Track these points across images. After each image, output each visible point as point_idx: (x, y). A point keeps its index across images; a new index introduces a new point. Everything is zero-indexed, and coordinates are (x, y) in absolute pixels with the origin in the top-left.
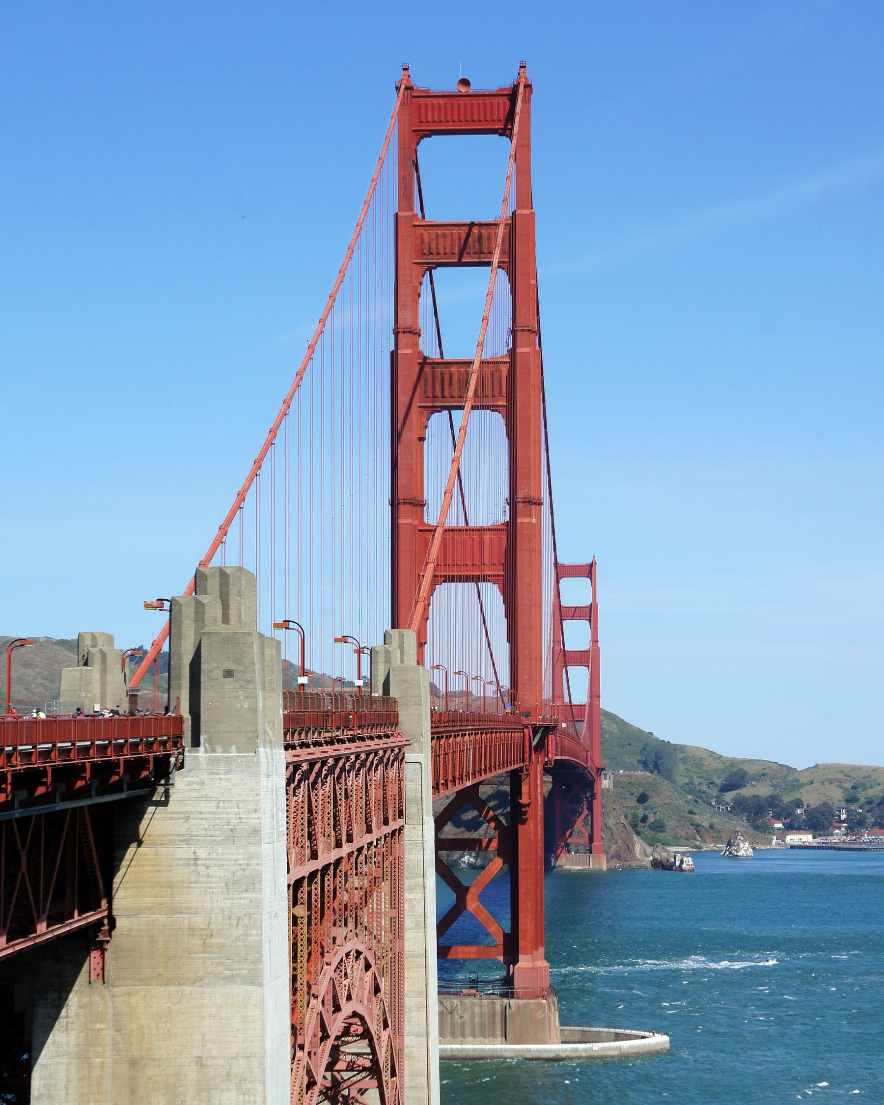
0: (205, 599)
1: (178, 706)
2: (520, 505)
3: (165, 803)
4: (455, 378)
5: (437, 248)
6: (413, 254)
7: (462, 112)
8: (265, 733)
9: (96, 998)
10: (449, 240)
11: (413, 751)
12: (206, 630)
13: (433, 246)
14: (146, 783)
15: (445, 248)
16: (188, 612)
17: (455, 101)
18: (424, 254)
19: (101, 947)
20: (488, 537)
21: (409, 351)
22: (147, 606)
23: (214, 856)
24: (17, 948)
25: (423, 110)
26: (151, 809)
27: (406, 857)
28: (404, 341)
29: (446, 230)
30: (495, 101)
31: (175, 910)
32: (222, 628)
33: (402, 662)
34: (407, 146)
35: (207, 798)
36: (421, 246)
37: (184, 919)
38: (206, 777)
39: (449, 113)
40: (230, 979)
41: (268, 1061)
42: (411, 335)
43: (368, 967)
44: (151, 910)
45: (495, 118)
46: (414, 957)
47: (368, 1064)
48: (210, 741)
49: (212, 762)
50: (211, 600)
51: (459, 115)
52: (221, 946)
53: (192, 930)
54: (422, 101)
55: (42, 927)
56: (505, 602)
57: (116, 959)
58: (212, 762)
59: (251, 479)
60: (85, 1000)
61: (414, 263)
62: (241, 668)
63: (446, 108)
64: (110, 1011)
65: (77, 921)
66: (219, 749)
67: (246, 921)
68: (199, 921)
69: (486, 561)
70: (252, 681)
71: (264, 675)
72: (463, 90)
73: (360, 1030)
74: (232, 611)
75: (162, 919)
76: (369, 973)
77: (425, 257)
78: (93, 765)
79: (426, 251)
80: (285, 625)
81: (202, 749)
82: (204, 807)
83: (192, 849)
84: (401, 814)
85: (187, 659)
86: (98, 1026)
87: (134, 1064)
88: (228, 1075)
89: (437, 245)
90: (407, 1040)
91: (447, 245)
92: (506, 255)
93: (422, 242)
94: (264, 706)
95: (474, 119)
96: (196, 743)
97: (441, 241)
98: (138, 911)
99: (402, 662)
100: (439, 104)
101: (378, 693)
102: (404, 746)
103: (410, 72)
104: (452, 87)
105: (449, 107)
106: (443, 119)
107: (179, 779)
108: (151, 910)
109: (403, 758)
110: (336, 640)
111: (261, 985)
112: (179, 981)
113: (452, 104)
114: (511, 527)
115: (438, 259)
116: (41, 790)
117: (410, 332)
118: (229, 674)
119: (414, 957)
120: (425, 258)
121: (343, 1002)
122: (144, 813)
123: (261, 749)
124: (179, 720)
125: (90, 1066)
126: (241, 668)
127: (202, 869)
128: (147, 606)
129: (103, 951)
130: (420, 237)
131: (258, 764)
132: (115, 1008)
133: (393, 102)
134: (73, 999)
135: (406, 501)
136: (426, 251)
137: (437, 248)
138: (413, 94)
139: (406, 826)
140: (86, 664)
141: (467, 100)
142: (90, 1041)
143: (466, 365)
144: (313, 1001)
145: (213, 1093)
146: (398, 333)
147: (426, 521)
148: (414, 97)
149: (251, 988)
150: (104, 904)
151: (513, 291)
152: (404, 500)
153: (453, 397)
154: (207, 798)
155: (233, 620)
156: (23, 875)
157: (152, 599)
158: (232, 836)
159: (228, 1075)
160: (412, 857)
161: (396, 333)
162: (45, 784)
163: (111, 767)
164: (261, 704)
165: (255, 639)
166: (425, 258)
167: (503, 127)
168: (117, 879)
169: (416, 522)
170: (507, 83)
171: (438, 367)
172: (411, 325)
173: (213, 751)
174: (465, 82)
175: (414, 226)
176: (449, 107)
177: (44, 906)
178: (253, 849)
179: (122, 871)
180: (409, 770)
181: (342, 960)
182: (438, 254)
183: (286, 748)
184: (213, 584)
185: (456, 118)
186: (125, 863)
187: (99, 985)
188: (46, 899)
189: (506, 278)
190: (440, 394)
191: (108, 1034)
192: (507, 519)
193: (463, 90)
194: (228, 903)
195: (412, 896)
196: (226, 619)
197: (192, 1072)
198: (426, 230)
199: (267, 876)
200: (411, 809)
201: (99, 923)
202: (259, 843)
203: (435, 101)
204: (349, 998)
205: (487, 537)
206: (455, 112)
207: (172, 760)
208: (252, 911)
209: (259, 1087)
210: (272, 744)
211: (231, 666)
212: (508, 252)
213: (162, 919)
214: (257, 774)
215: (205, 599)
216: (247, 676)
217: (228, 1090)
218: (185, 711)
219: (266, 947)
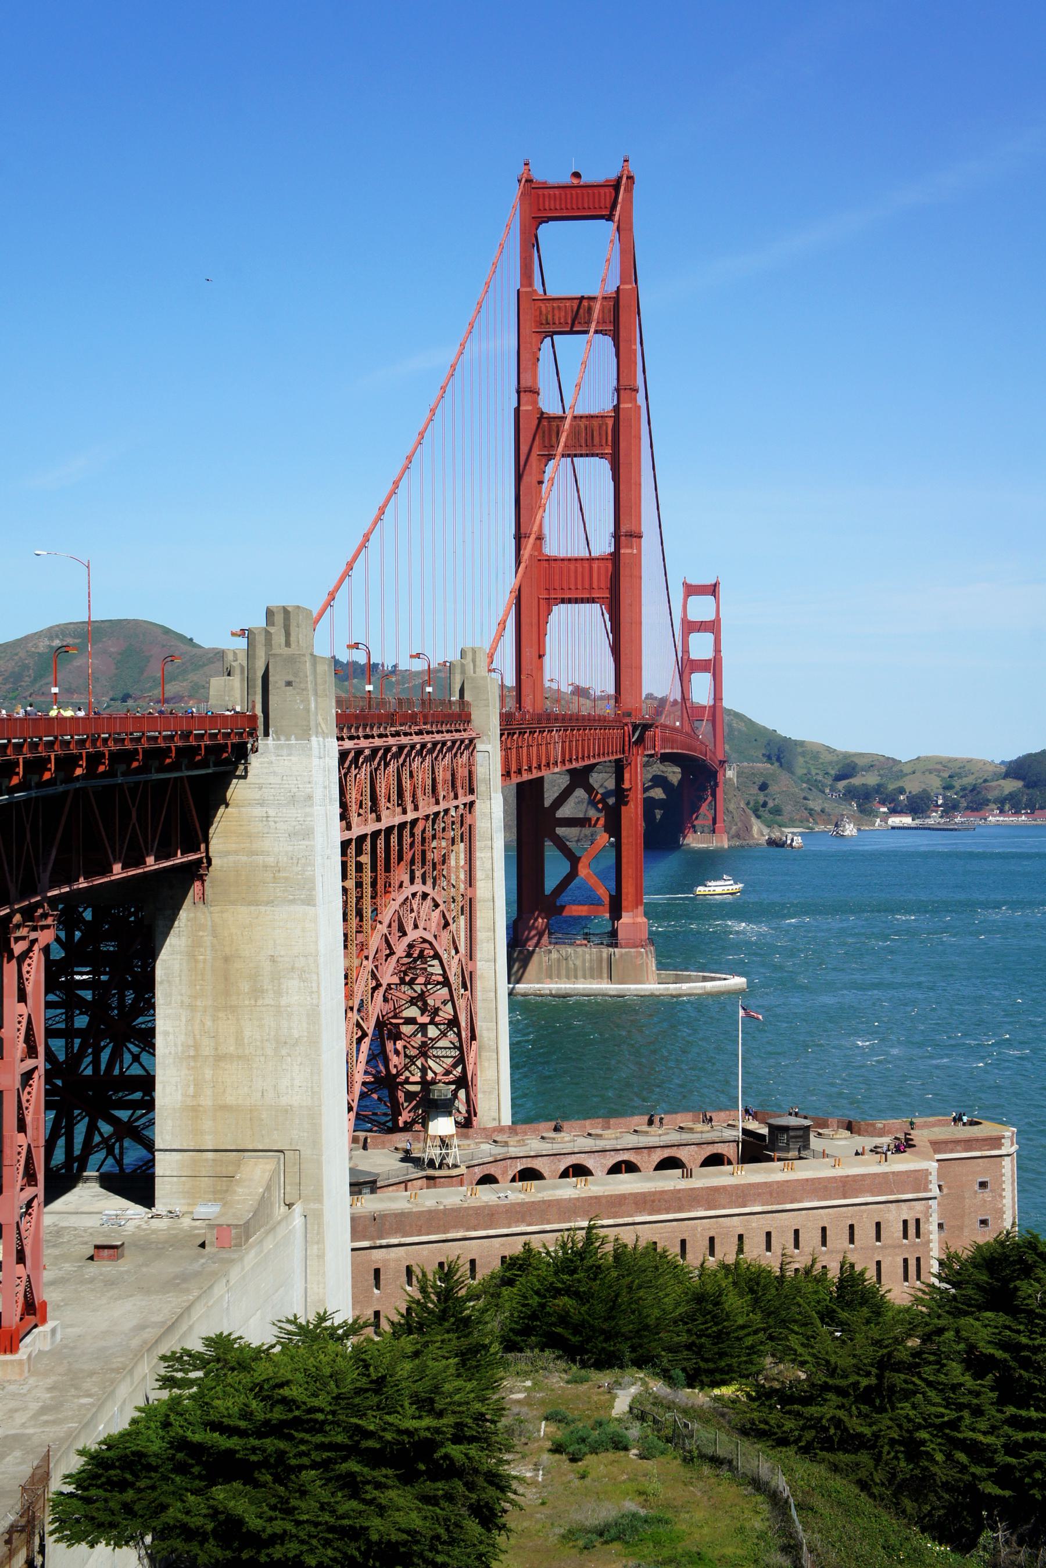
0: (272, 630)
1: (254, 707)
2: (623, 538)
3: (245, 777)
8: (318, 725)
9: (199, 914)
11: (483, 743)
12: (273, 652)
13: (550, 317)
14: (227, 762)
15: (560, 319)
16: (260, 639)
17: (568, 191)
19: (201, 879)
21: (530, 408)
22: (233, 634)
23: (280, 815)
24: (130, 874)
25: (541, 200)
26: (235, 781)
27: (478, 825)
30: (602, 191)
31: (253, 853)
32: (286, 651)
33: (475, 672)
35: (274, 773)
37: (260, 859)
38: (273, 758)
39: (563, 202)
40: (293, 902)
41: (321, 960)
43: (437, 905)
44: (236, 852)
45: (602, 205)
46: (485, 901)
47: (441, 979)
48: (276, 732)
49: (278, 747)
50: (278, 632)
51: (571, 203)
52: (286, 879)
53: (265, 866)
54: (540, 192)
55: (150, 860)
57: (212, 887)
58: (278, 747)
59: (375, 524)
60: (192, 915)
62: (298, 680)
63: (561, 199)
64: (209, 923)
65: (180, 859)
66: (283, 738)
67: (303, 861)
68: (271, 860)
69: (595, 585)
70: (306, 689)
71: (316, 684)
72: (575, 181)
73: (432, 953)
74: (293, 639)
75: (244, 859)
76: (438, 911)
78: (178, 748)
80: (356, 646)
81: (270, 738)
82: (272, 779)
83: (265, 809)
84: (472, 791)
85: (260, 673)
86: (201, 933)
87: (226, 959)
88: (293, 968)
90: (479, 964)
94: (316, 708)
96: (266, 734)
97: (556, 312)
98: (228, 853)
99: (475, 672)
101: (455, 698)
102: (474, 739)
103: (531, 167)
104: (566, 179)
105: (563, 197)
107: (254, 760)
108: (236, 852)
109: (475, 748)
110: (412, 656)
111: (314, 905)
112: (256, 903)
113: (566, 195)
116: (135, 764)
118: (289, 684)
119: (485, 901)
121: (409, 927)
122: (230, 784)
123: (314, 739)
124: (254, 717)
125: (196, 961)
126: (298, 680)
127: (272, 824)
128: (233, 634)
129: (203, 881)
131: (311, 749)
132: (212, 921)
133: (515, 192)
134: (183, 914)
139: (477, 801)
140: (229, 675)
142: (196, 944)
144: (379, 926)
145: (282, 980)
149: (307, 907)
150: (203, 846)
151: (618, 355)
154: (274, 773)
155: (293, 645)
156: (134, 825)
157: (237, 630)
158: (293, 800)
159: (293, 968)
160: (483, 825)
161: (518, 392)
162: (138, 760)
163: (195, 750)
164: (313, 706)
165: (308, 658)
168: (211, 831)
169: (536, 554)
170: (613, 175)
173: (279, 739)
174: (577, 175)
176: (563, 197)
177: (152, 847)
178: (308, 810)
179: (214, 826)
180: (479, 757)
181: (407, 898)
183: (340, 739)
184: (279, 619)
186: (217, 819)
187: (201, 906)
188: (153, 841)
189: (611, 343)
191: (208, 940)
193: (575, 181)
194: (290, 848)
195: (482, 855)
196: (288, 644)
197: (267, 966)
199: (319, 829)
200: (480, 787)
201: (200, 861)
202: (312, 806)
203: (551, 192)
204: (416, 927)
205: (595, 565)
207: (249, 746)
208: (307, 854)
209: (315, 977)
210: (325, 735)
211: (290, 678)
213: (244, 859)
214: (310, 756)
215: (272, 630)
216: (302, 686)
217: (293, 978)
218: (259, 712)
219: (319, 880)
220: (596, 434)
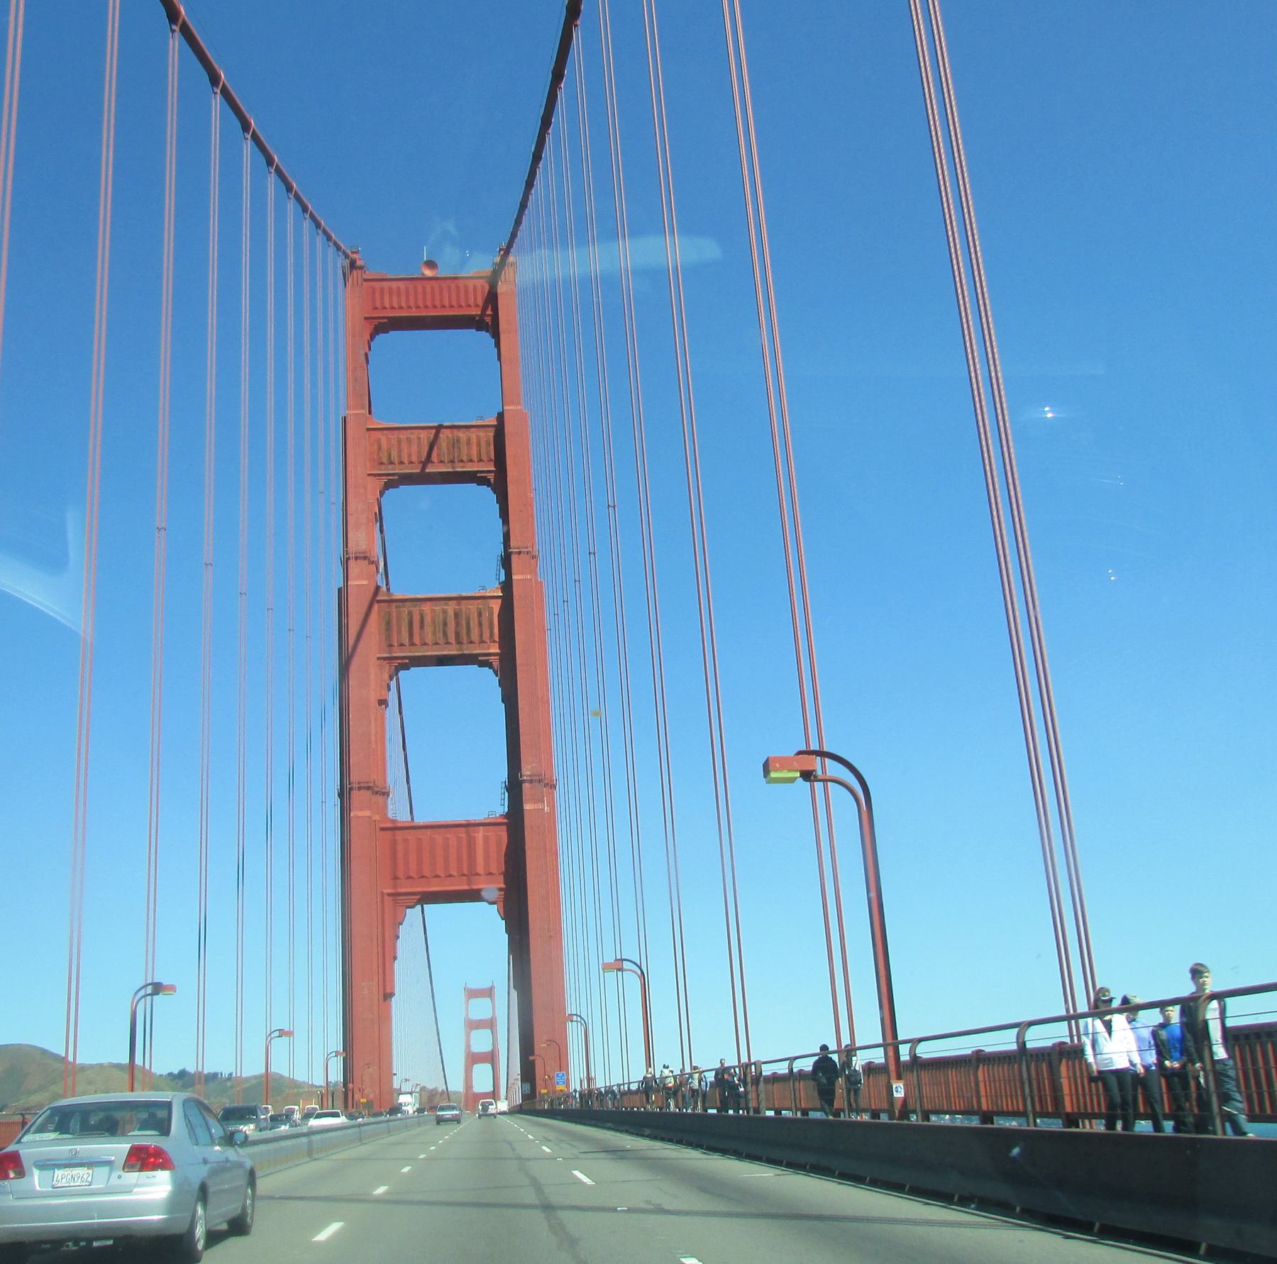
2: (526, 786)
4: (428, 619)
5: (400, 456)
13: (394, 454)
15: (409, 455)
18: (382, 463)
20: (481, 835)
25: (377, 296)
29: (412, 434)
36: (378, 453)
39: (412, 298)
54: (377, 285)
56: (509, 929)
61: (369, 475)
69: (480, 869)
77: (383, 467)
79: (385, 460)
89: (400, 451)
91: (413, 452)
92: (492, 463)
93: (380, 448)
97: (404, 445)
100: (399, 288)
105: (411, 291)
106: (404, 305)
113: (415, 288)
114: (515, 819)
115: (401, 470)
120: (383, 468)
135: (362, 785)
136: (385, 460)
137: (400, 456)
138: (365, 277)
141: (434, 283)
143: (443, 602)
146: (348, 559)
147: (390, 815)
148: (365, 280)
152: (359, 783)
153: (425, 644)
161: (346, 563)
166: (383, 468)
167: (480, 313)
169: (377, 817)
171: (404, 606)
175: (369, 430)
176: (411, 291)
182: (402, 463)
185: (421, 304)
190: (407, 640)
192: (506, 810)
203: (394, 285)
205: (480, 834)
212: (493, 458)
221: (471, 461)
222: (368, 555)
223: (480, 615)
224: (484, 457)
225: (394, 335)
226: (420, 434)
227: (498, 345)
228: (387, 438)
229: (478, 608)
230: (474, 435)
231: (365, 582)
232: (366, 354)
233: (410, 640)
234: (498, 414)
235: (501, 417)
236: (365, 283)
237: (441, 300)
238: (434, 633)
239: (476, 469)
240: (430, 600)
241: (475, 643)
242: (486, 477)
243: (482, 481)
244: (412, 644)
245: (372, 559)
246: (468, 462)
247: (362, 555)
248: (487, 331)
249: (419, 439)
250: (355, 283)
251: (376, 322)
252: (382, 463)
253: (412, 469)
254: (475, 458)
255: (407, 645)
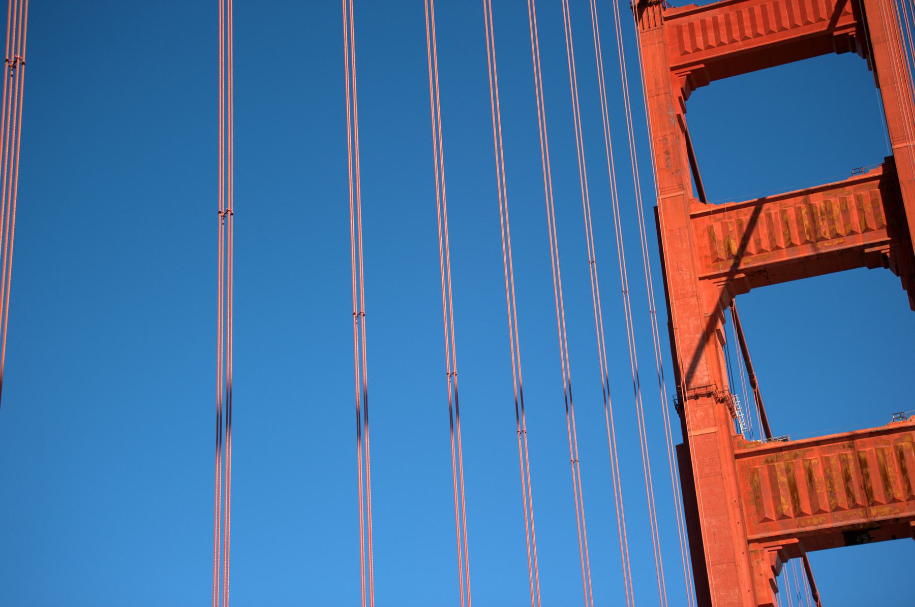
4: (819, 475)
6: (698, 264)
7: (759, 20)
10: (765, 228)
25: (686, 36)
28: (700, 414)
34: (662, 92)
39: (735, 27)
42: (711, 400)
51: (754, 26)
61: (701, 279)
92: (884, 231)
95: (784, 25)
105: (733, 18)
117: (709, 395)
130: (706, 234)
138: (665, 14)
148: (666, 19)
172: (709, 381)
175: (693, 217)
198: (716, 220)
203: (708, 16)
206: (747, 23)
212: (885, 223)
220: (893, 470)
221: (852, 233)
222: (713, 389)
223: (901, 457)
224: (872, 225)
225: (716, 86)
226: (769, 209)
227: (873, 66)
228: (722, 223)
229: (896, 447)
230: (852, 195)
231: (713, 430)
232: (679, 116)
233: (795, 508)
234: (885, 158)
235: (890, 164)
236: (665, 23)
237: (779, 20)
238: (832, 494)
239: (861, 243)
240: (817, 443)
241: (900, 501)
242: (880, 251)
243: (874, 261)
244: (800, 514)
245: (720, 396)
246: (848, 235)
247: (703, 391)
248: (854, 51)
249: (769, 216)
250: (652, 25)
251: (688, 71)
252: (718, 260)
253: (764, 260)
254: (857, 228)
255: (792, 516)
